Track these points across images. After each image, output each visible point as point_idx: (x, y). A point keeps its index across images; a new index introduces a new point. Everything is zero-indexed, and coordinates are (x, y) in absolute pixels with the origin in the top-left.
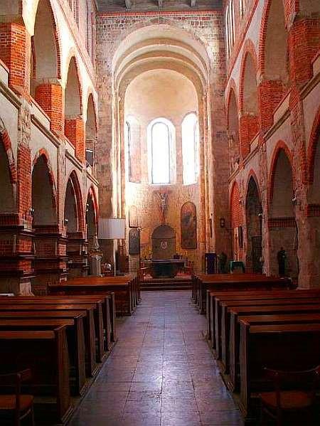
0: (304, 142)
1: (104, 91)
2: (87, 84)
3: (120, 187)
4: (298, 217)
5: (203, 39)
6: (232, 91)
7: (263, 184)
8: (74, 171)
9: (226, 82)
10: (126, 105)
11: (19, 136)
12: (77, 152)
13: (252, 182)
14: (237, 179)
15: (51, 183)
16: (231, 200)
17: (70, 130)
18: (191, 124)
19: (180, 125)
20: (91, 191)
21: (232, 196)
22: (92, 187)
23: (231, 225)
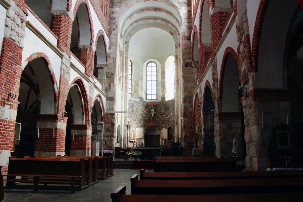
0: (248, 36)
1: (112, 36)
2: (97, 26)
3: (123, 100)
4: (244, 103)
5: (177, 5)
6: (195, 33)
7: (215, 92)
8: (80, 80)
9: (191, 31)
10: (129, 49)
11: (6, 32)
12: (87, 70)
13: (207, 88)
14: (198, 91)
15: (53, 82)
16: (195, 108)
17: (78, 51)
18: (171, 61)
19: (164, 63)
20: (98, 98)
21: (195, 105)
22: (99, 96)
23: (194, 125)
